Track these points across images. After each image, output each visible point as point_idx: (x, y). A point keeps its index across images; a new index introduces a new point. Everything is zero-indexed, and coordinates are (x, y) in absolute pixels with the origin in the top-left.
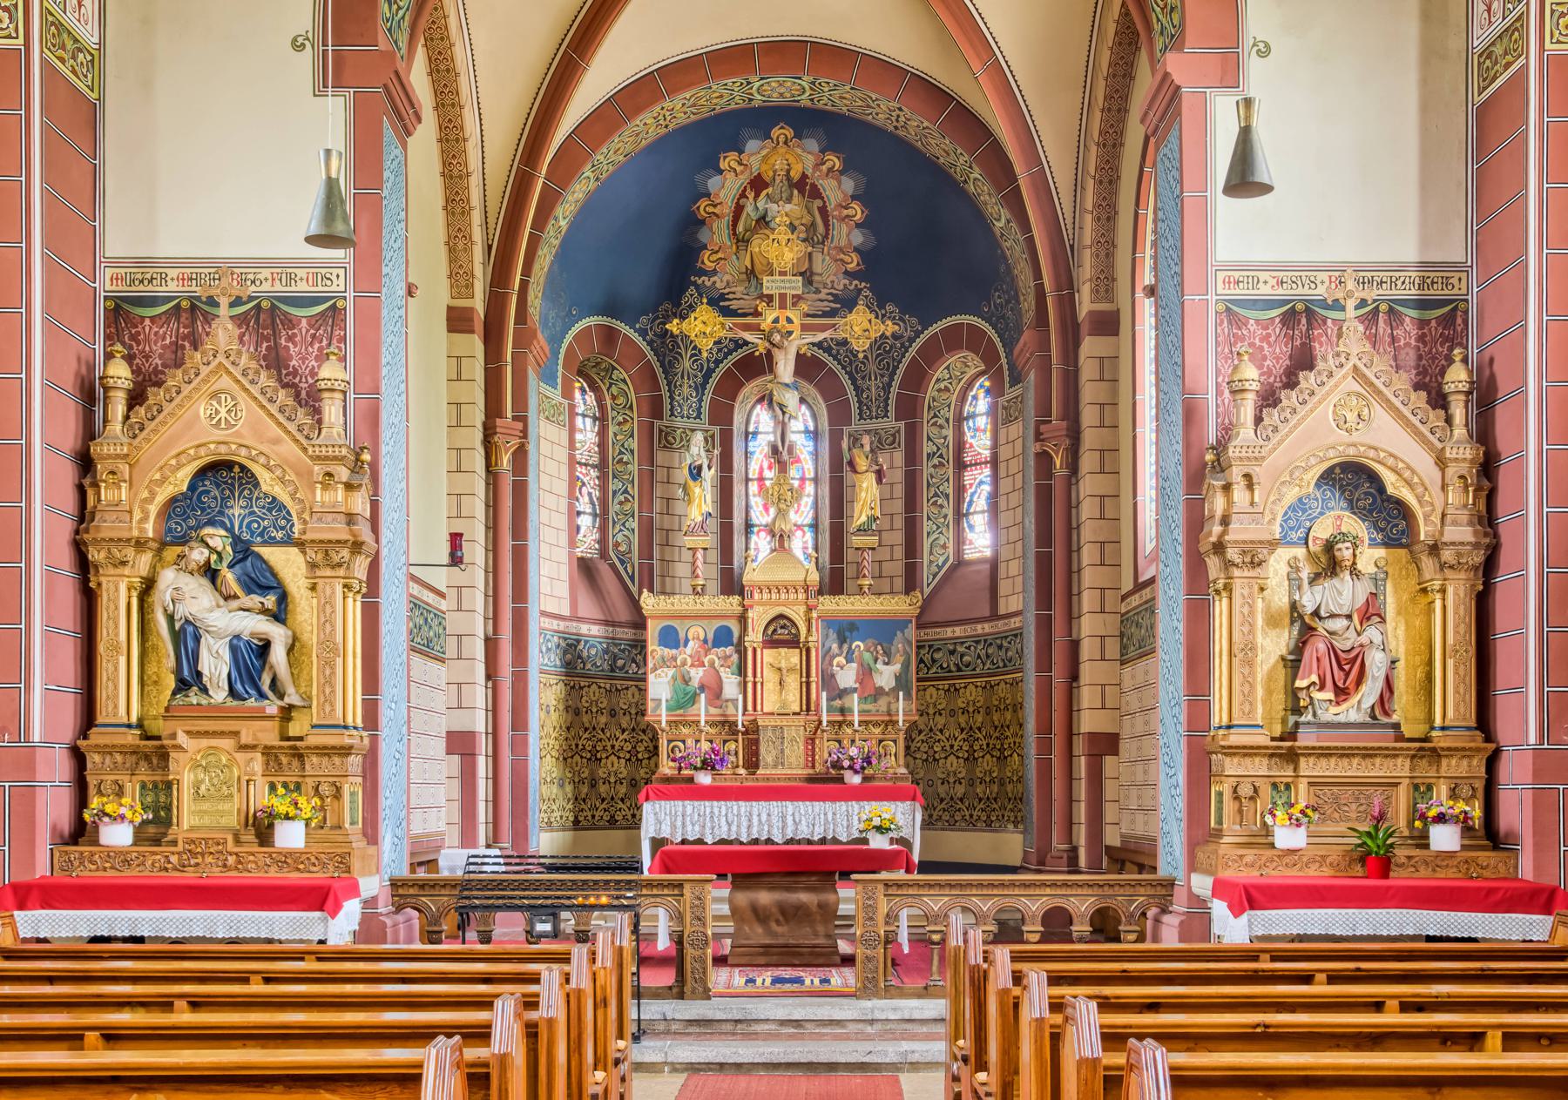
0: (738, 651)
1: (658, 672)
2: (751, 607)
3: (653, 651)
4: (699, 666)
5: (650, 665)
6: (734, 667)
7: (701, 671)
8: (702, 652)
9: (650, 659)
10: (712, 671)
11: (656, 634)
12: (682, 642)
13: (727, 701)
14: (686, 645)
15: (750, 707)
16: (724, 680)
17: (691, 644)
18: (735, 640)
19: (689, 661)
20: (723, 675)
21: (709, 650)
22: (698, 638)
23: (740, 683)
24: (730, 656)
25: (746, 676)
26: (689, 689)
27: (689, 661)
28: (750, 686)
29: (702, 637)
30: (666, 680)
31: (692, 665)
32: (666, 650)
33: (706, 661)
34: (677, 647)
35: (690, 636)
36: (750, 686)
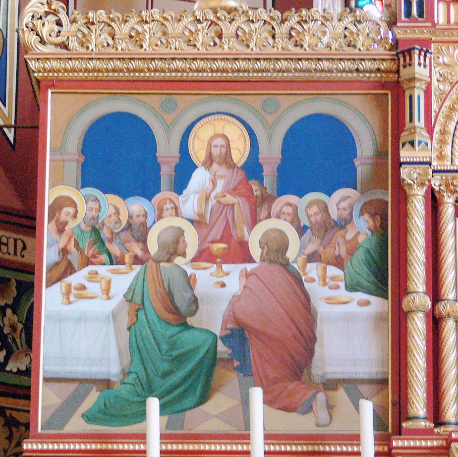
0: (376, 210)
1: (75, 279)
2: (425, 46)
3: (57, 206)
4: (229, 257)
5: (49, 255)
6: (359, 263)
7: (234, 275)
8: (242, 207)
9: (47, 229)
10: (276, 269)
11: (74, 144)
12: (165, 181)
13: (331, 385)
14: (180, 185)
15: (419, 405)
16: (322, 308)
17: (200, 178)
18: (362, 169)
19: (192, 241)
20: (317, 291)
21: (267, 199)
22: (227, 160)
23: (380, 318)
24: (343, 224)
25: (402, 289)
26: (188, 339)
27: (192, 241)
28: (418, 326)
29: (240, 152)
30: (103, 307)
31: (204, 256)
32: (110, 201)
33: (254, 240)
34: (148, 190)
35: (198, 150)
36: (418, 326)
